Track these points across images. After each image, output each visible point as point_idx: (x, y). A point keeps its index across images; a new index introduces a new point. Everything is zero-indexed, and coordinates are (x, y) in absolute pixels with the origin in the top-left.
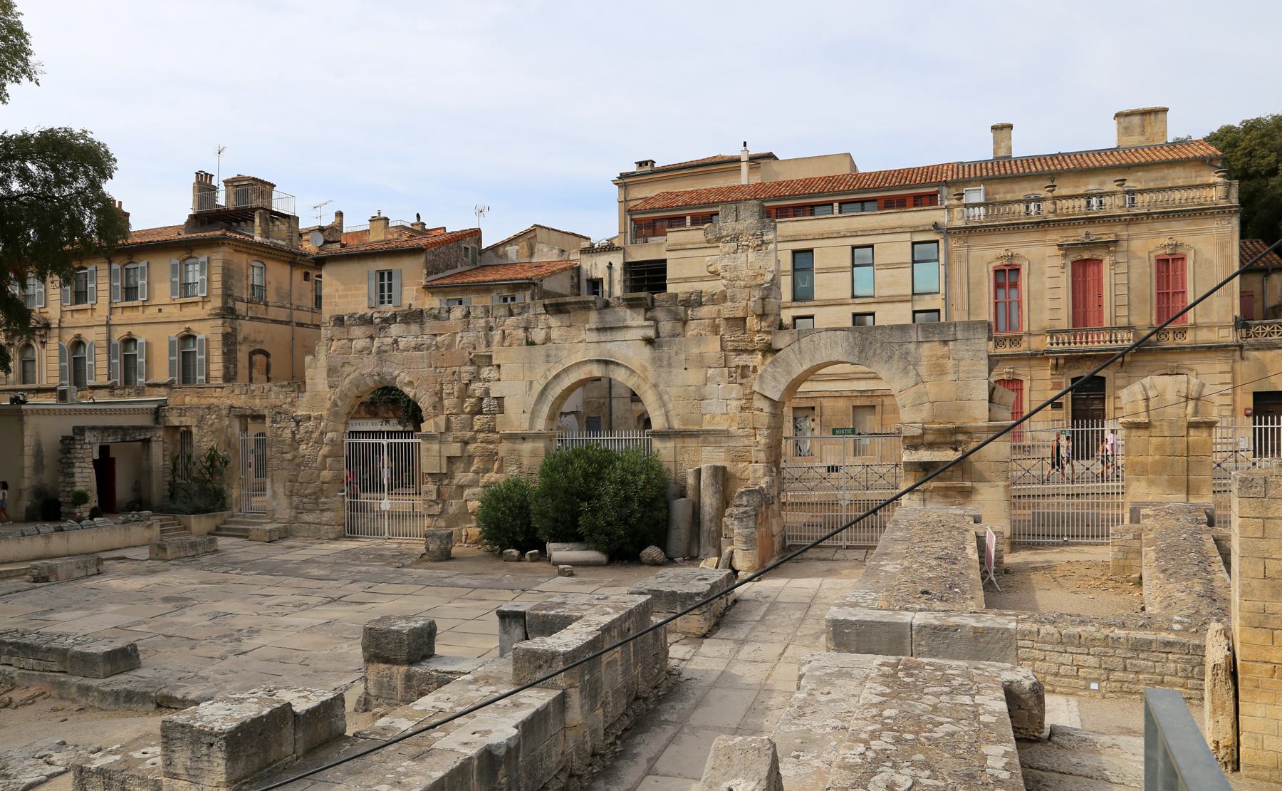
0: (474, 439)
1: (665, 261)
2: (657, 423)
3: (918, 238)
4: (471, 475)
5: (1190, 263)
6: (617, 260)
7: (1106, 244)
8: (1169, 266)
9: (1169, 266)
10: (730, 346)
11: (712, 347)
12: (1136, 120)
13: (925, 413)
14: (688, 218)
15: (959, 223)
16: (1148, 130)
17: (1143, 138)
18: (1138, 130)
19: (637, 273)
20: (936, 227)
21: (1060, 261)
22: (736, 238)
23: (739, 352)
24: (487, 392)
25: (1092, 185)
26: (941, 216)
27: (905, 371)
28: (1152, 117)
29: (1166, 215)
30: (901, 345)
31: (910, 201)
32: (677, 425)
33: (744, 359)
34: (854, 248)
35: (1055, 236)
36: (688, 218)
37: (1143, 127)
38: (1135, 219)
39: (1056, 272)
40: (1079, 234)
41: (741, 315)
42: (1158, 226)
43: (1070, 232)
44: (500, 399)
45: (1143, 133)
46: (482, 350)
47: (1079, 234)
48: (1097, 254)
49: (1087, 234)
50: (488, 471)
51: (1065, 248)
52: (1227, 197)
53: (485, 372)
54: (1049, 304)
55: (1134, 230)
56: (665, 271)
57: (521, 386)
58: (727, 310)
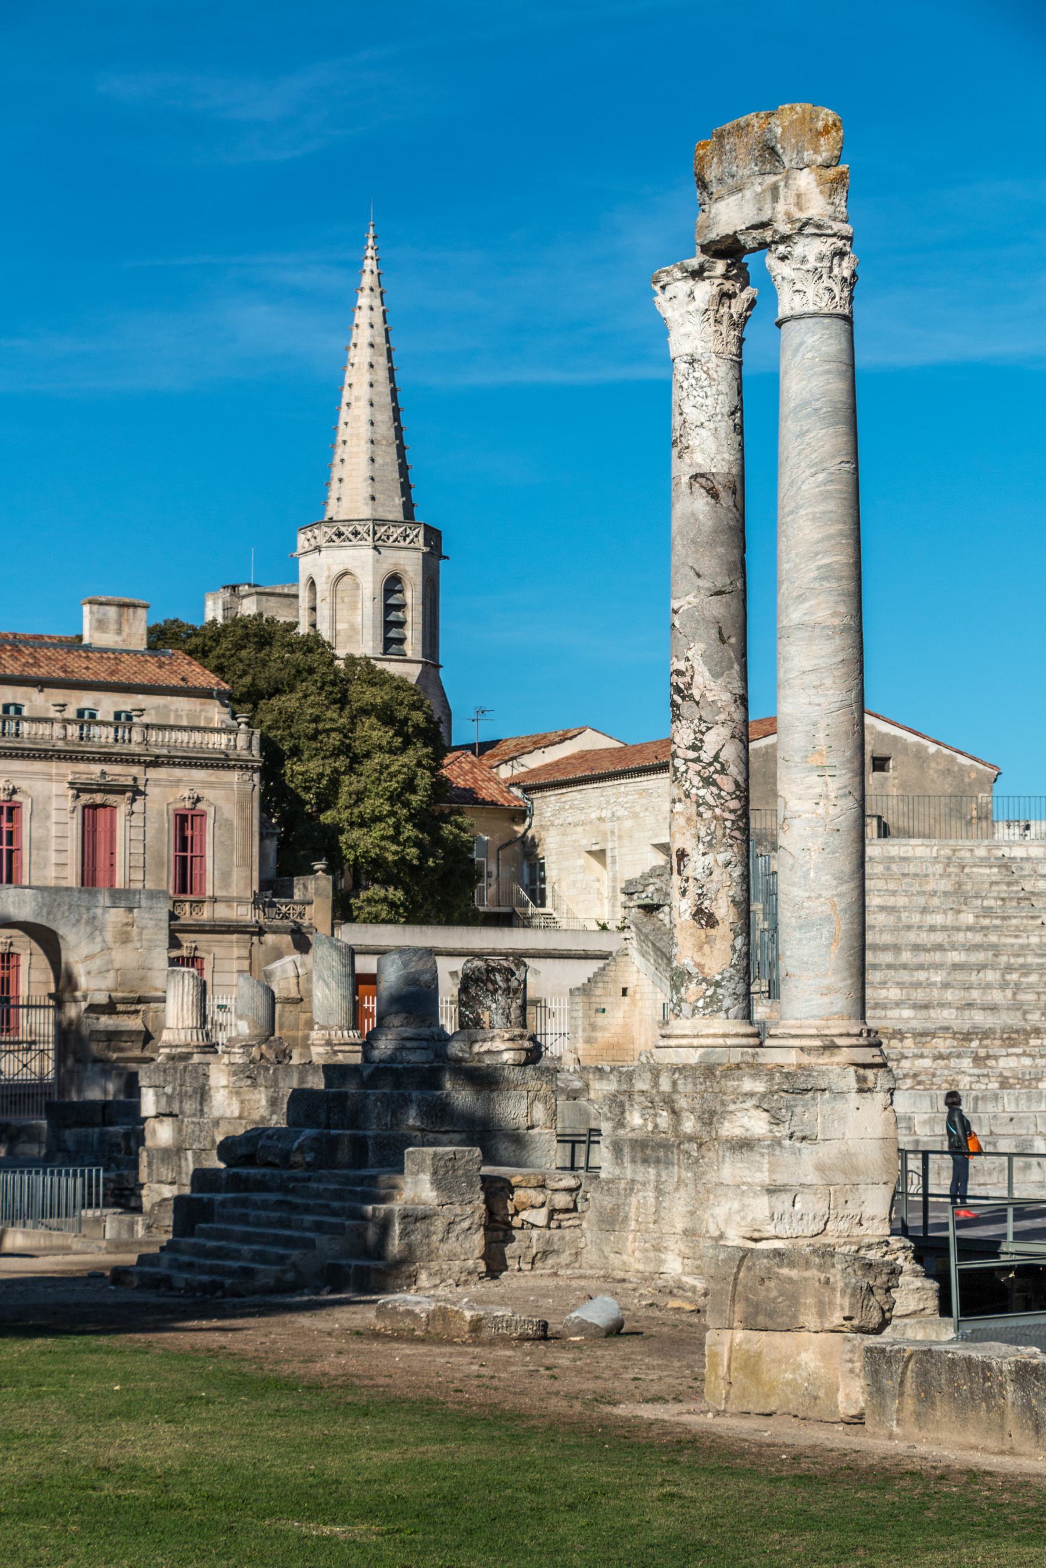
5: (210, 822)
7: (120, 790)
8: (186, 824)
9: (186, 824)
12: (112, 612)
13: (109, 981)
16: (126, 629)
17: (119, 639)
18: (113, 626)
25: (86, 700)
27: (91, 937)
28: (131, 610)
29: (190, 762)
30: (88, 909)
38: (156, 762)
39: (65, 817)
42: (178, 773)
43: (82, 767)
45: (119, 631)
48: (111, 799)
49: (103, 774)
51: (80, 789)
52: (250, 747)
54: (53, 858)
55: (153, 773)
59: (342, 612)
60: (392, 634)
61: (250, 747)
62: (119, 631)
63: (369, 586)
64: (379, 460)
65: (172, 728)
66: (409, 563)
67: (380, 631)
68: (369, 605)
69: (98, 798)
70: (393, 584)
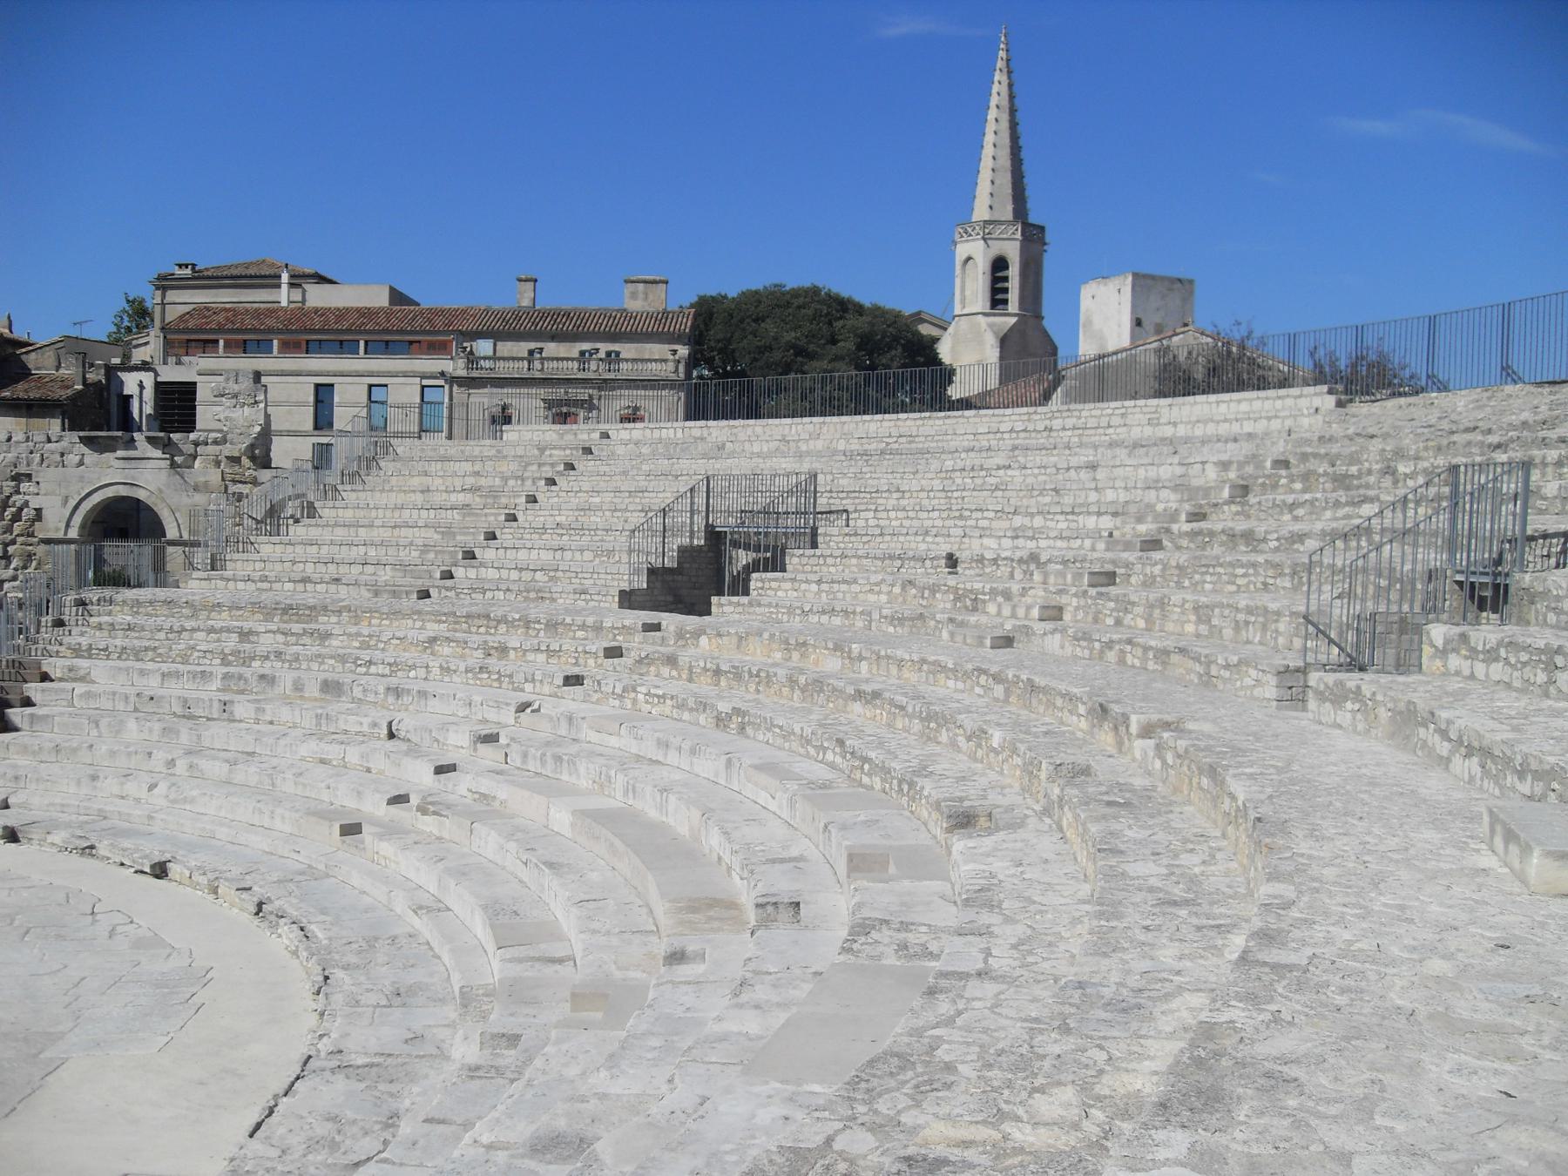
0: (13, 542)
1: (195, 383)
2: (172, 533)
3: (425, 382)
4: (10, 572)
6: (148, 379)
10: (228, 477)
11: (214, 476)
14: (221, 343)
15: (462, 373)
16: (651, 297)
18: (641, 296)
19: (165, 393)
20: (443, 374)
21: (542, 412)
22: (235, 396)
23: (234, 481)
24: (26, 504)
25: (586, 346)
26: (447, 366)
31: (425, 346)
32: (186, 536)
33: (239, 488)
34: (370, 386)
35: (542, 392)
36: (221, 343)
37: (646, 294)
38: (604, 385)
40: (559, 393)
41: (237, 454)
44: (39, 511)
45: (646, 299)
46: (23, 469)
47: (559, 393)
50: (25, 567)
52: (677, 370)
53: (24, 486)
56: (195, 393)
57: (58, 501)
58: (228, 450)
59: (968, 284)
60: (999, 296)
61: (677, 370)
62: (646, 299)
63: (982, 266)
64: (997, 182)
65: (642, 360)
66: (1012, 251)
67: (988, 295)
68: (980, 276)
69: (564, 410)
70: (999, 264)
